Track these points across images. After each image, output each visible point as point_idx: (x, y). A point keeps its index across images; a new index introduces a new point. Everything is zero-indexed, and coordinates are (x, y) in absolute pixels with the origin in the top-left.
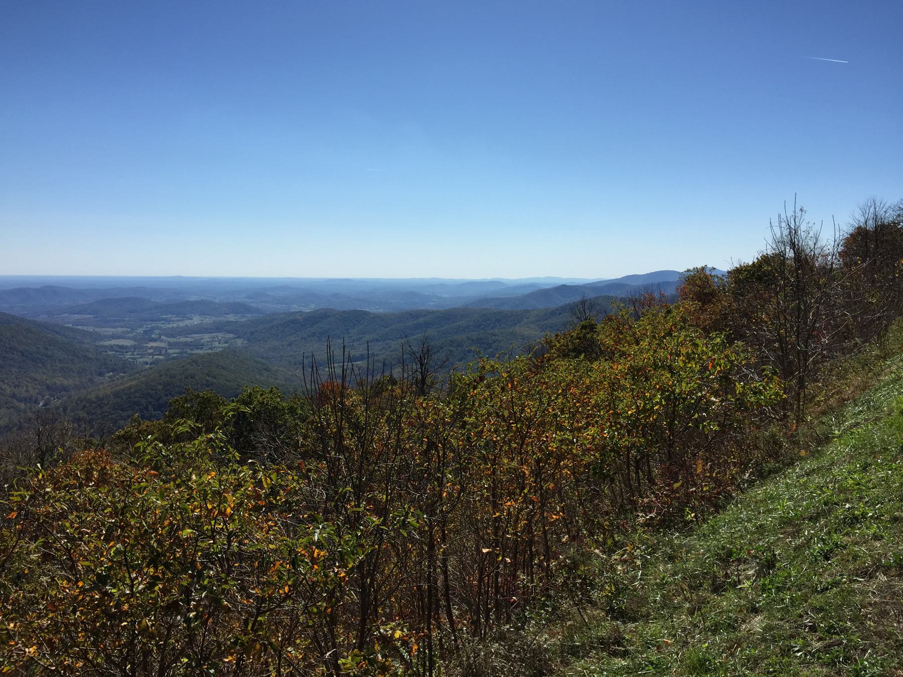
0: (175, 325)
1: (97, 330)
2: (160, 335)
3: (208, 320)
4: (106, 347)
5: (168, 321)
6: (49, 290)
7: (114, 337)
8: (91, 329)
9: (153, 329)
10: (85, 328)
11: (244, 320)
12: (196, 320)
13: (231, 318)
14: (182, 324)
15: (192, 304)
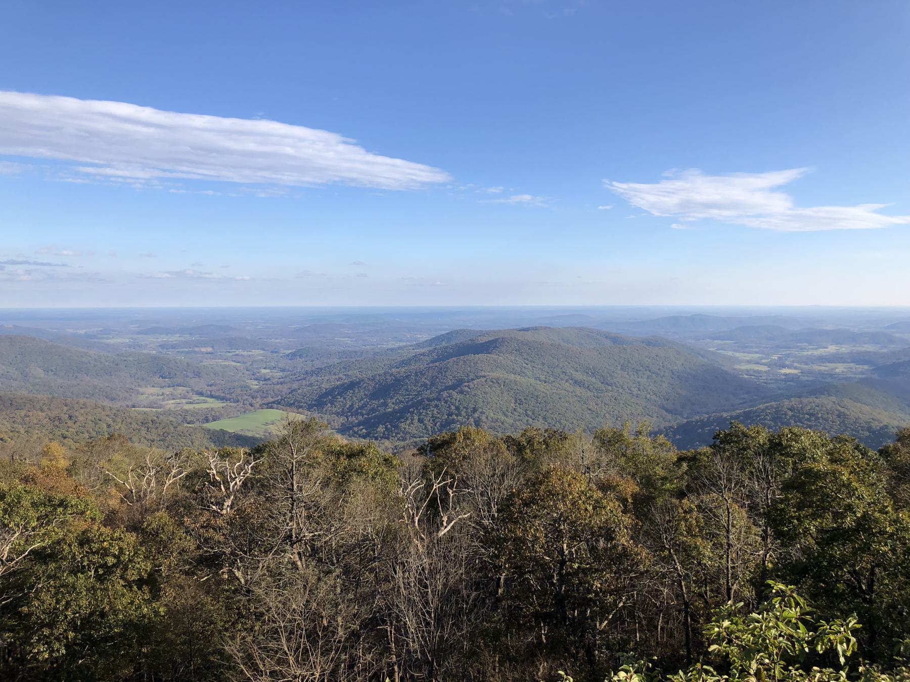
0: (809, 353)
1: (738, 355)
2: (793, 361)
3: (845, 349)
4: (740, 370)
5: (802, 349)
6: (697, 319)
7: (749, 362)
8: (730, 353)
9: (788, 356)
10: (725, 353)
11: (884, 351)
12: (832, 349)
13: (870, 348)
14: (816, 353)
15: (827, 333)
